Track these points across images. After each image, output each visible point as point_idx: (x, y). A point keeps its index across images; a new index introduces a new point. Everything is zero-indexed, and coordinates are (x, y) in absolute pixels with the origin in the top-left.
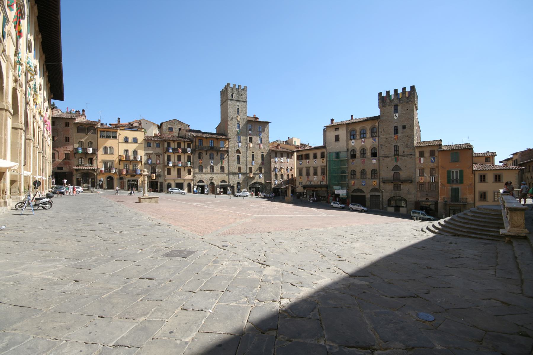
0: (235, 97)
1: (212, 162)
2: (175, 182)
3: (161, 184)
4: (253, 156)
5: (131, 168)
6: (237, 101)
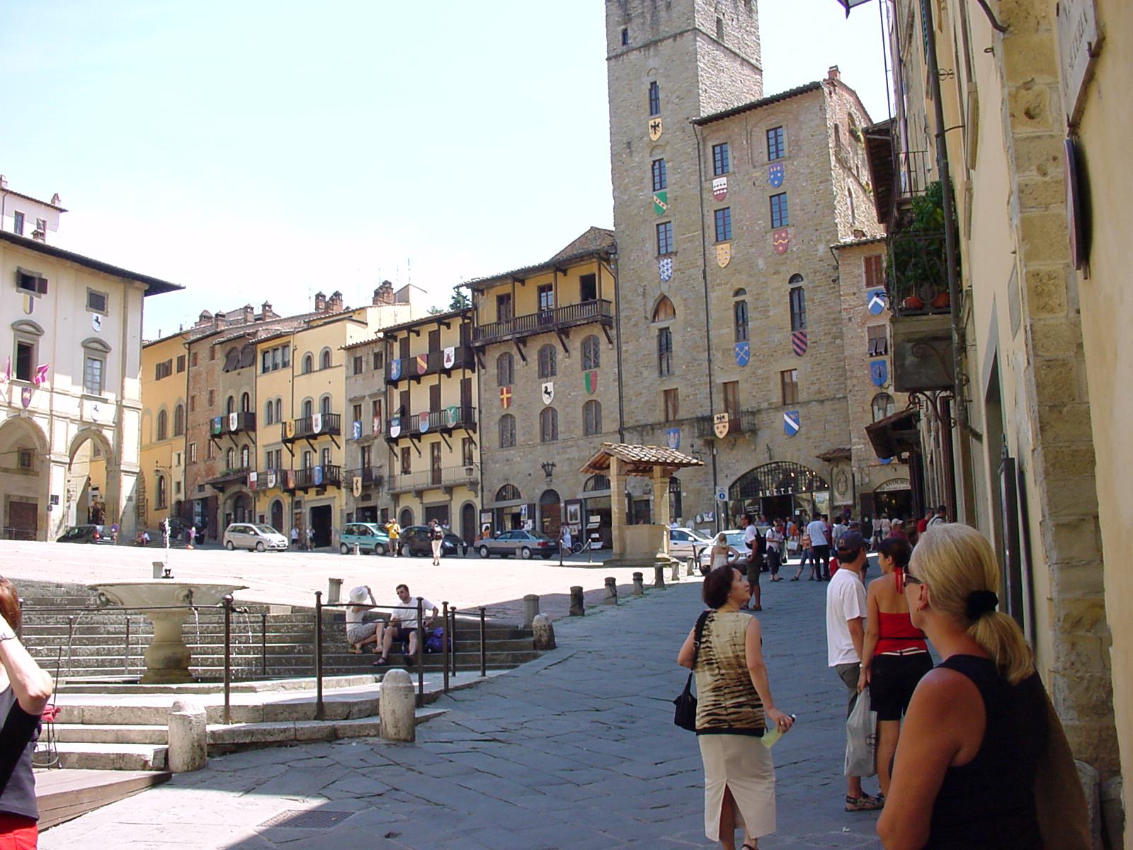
0: (636, 38)
1: (546, 392)
2: (424, 502)
3: (384, 511)
4: (740, 310)
5: (316, 460)
6: (646, 46)
